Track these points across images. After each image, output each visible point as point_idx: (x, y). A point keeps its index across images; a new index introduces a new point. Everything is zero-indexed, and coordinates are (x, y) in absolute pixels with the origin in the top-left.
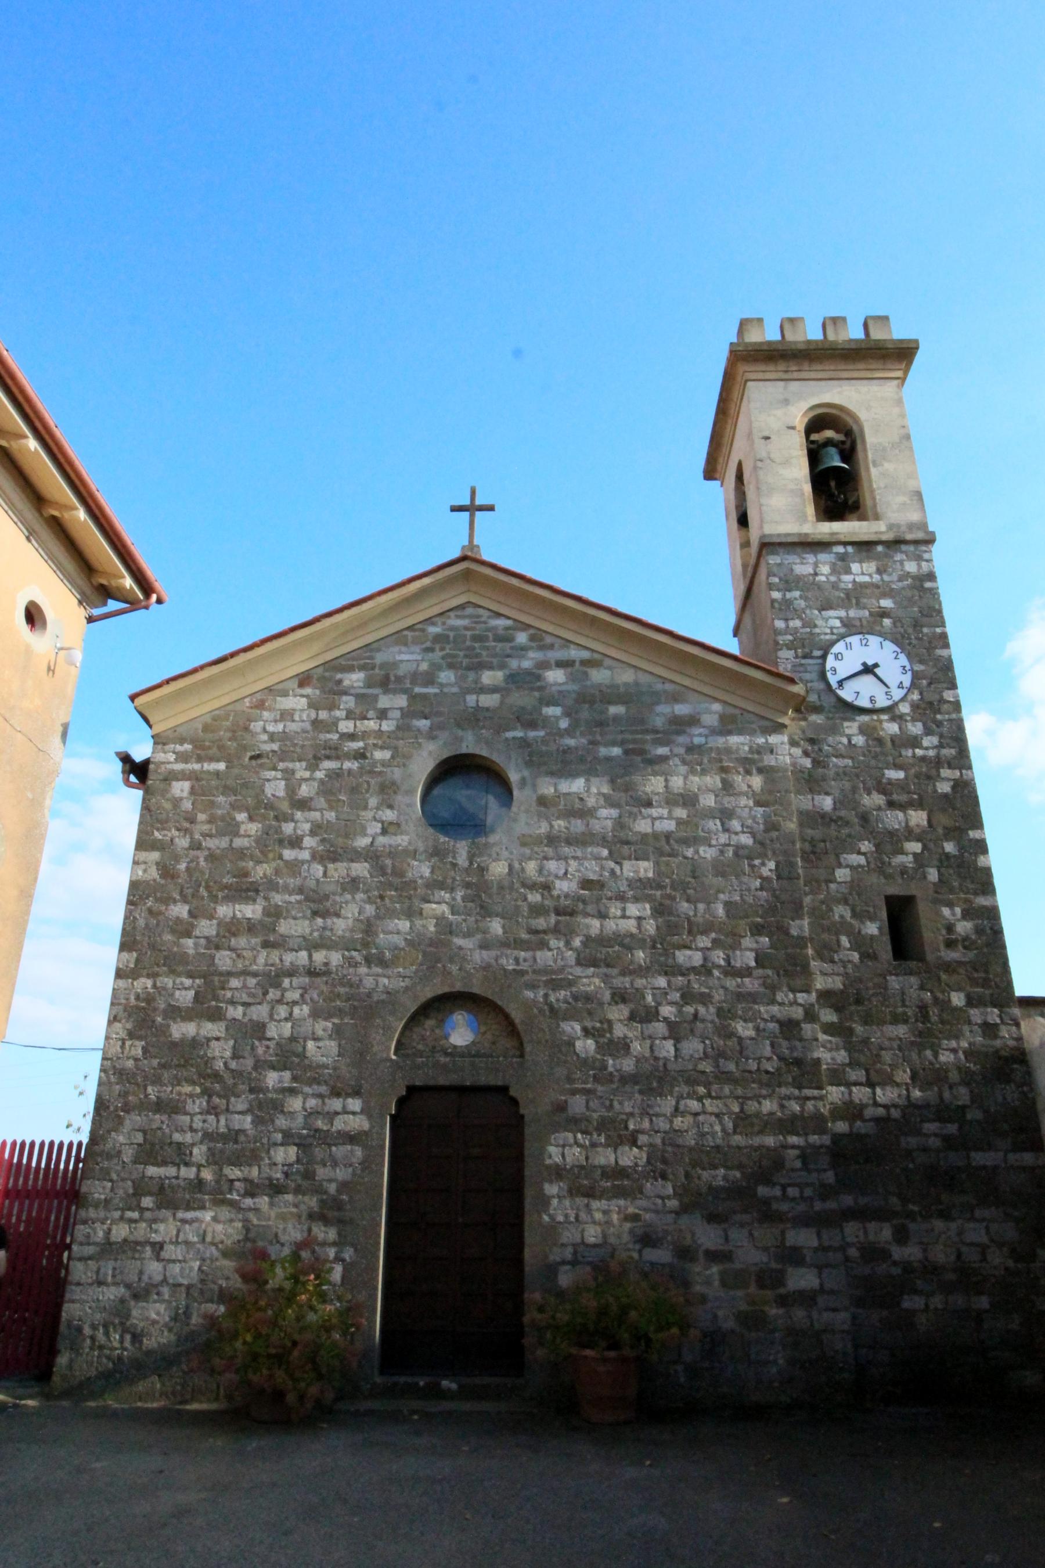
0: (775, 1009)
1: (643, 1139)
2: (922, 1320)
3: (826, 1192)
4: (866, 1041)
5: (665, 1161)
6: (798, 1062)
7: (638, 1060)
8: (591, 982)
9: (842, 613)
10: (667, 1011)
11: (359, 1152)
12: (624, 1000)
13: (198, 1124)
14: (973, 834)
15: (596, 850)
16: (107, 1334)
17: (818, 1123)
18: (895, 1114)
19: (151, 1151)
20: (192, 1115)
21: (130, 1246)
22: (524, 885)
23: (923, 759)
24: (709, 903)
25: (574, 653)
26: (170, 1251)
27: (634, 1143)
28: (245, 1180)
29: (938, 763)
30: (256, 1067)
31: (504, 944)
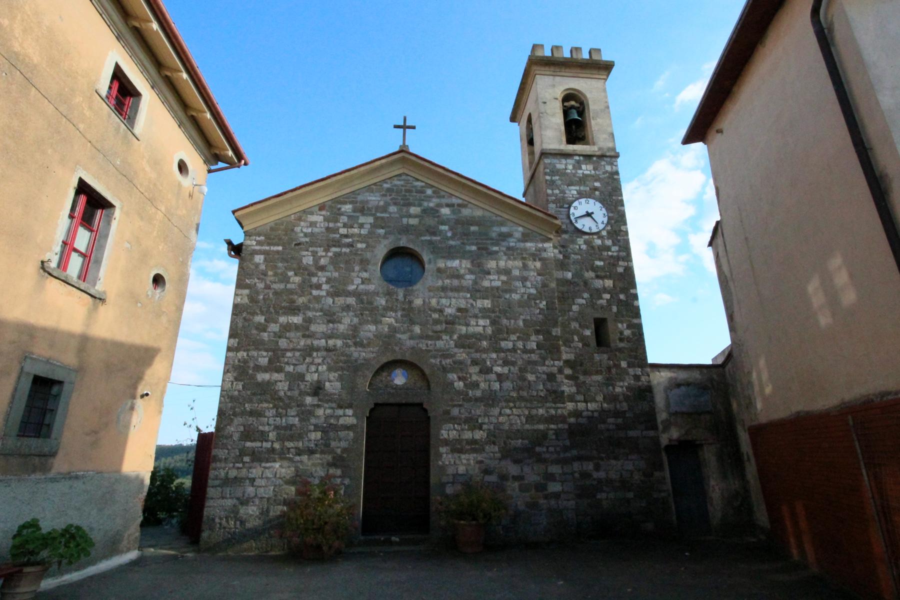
0: (545, 368)
1: (485, 427)
2: (604, 503)
3: (566, 449)
4: (584, 382)
5: (495, 436)
6: (555, 392)
7: (483, 391)
8: (461, 355)
9: (578, 188)
10: (498, 369)
11: (351, 434)
12: (477, 364)
13: (271, 421)
14: (632, 291)
15: (464, 294)
16: (227, 521)
17: (563, 419)
18: (596, 414)
19: (248, 434)
20: (268, 418)
21: (237, 481)
22: (431, 310)
23: (612, 256)
24: (516, 320)
25: (454, 201)
26: (258, 482)
27: (481, 428)
28: (296, 448)
29: (618, 258)
30: (300, 395)
31: (421, 337)
